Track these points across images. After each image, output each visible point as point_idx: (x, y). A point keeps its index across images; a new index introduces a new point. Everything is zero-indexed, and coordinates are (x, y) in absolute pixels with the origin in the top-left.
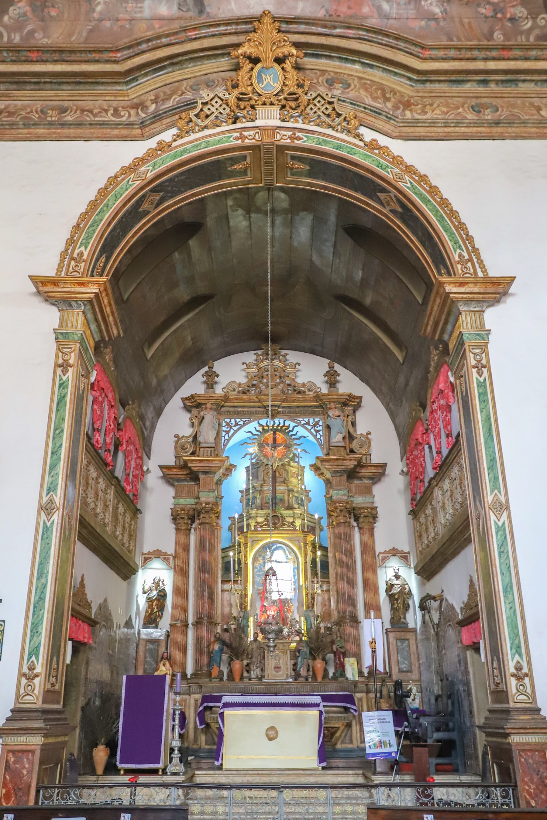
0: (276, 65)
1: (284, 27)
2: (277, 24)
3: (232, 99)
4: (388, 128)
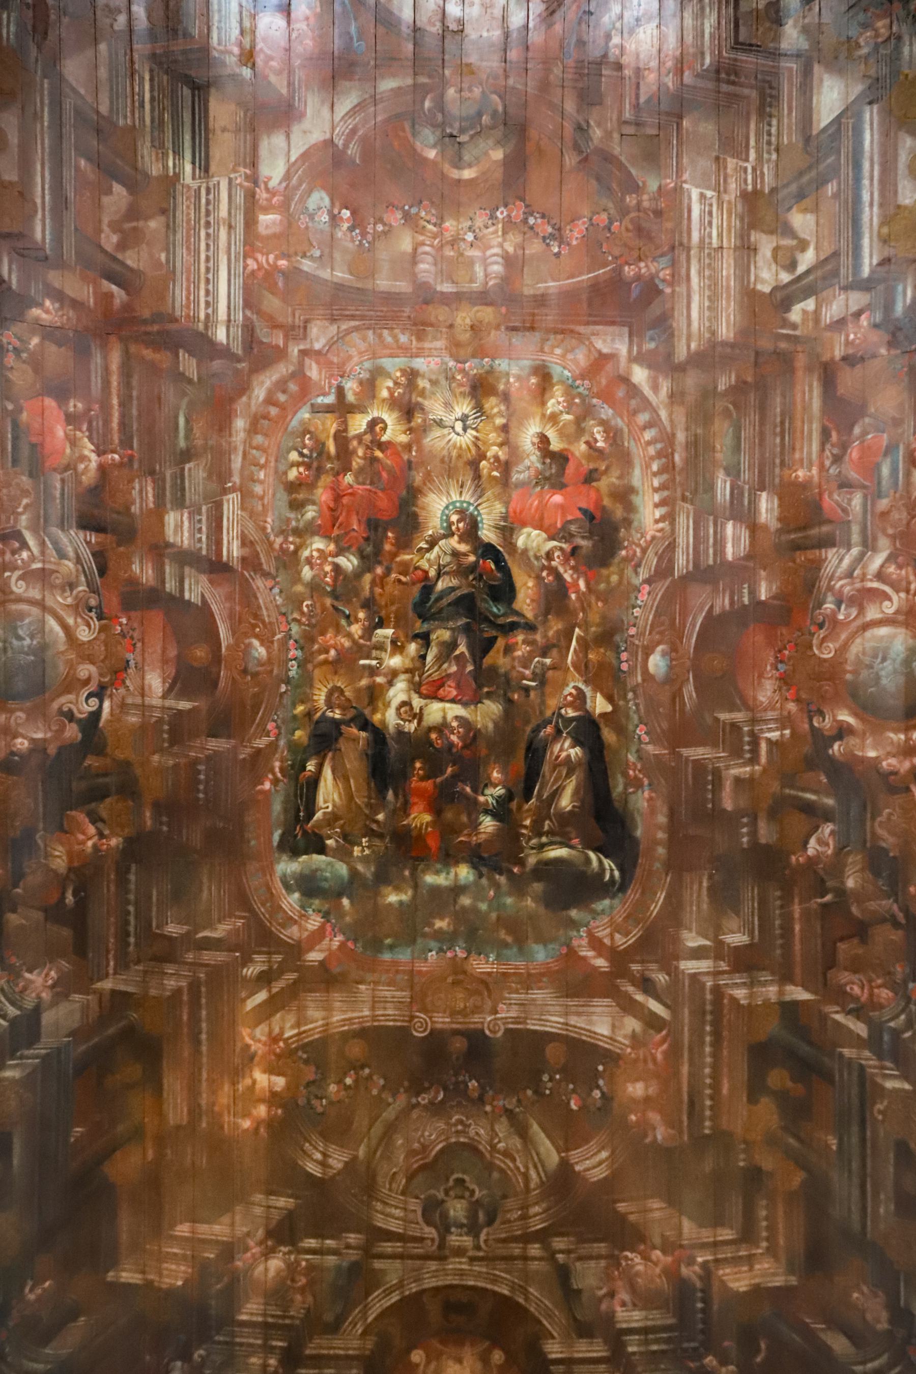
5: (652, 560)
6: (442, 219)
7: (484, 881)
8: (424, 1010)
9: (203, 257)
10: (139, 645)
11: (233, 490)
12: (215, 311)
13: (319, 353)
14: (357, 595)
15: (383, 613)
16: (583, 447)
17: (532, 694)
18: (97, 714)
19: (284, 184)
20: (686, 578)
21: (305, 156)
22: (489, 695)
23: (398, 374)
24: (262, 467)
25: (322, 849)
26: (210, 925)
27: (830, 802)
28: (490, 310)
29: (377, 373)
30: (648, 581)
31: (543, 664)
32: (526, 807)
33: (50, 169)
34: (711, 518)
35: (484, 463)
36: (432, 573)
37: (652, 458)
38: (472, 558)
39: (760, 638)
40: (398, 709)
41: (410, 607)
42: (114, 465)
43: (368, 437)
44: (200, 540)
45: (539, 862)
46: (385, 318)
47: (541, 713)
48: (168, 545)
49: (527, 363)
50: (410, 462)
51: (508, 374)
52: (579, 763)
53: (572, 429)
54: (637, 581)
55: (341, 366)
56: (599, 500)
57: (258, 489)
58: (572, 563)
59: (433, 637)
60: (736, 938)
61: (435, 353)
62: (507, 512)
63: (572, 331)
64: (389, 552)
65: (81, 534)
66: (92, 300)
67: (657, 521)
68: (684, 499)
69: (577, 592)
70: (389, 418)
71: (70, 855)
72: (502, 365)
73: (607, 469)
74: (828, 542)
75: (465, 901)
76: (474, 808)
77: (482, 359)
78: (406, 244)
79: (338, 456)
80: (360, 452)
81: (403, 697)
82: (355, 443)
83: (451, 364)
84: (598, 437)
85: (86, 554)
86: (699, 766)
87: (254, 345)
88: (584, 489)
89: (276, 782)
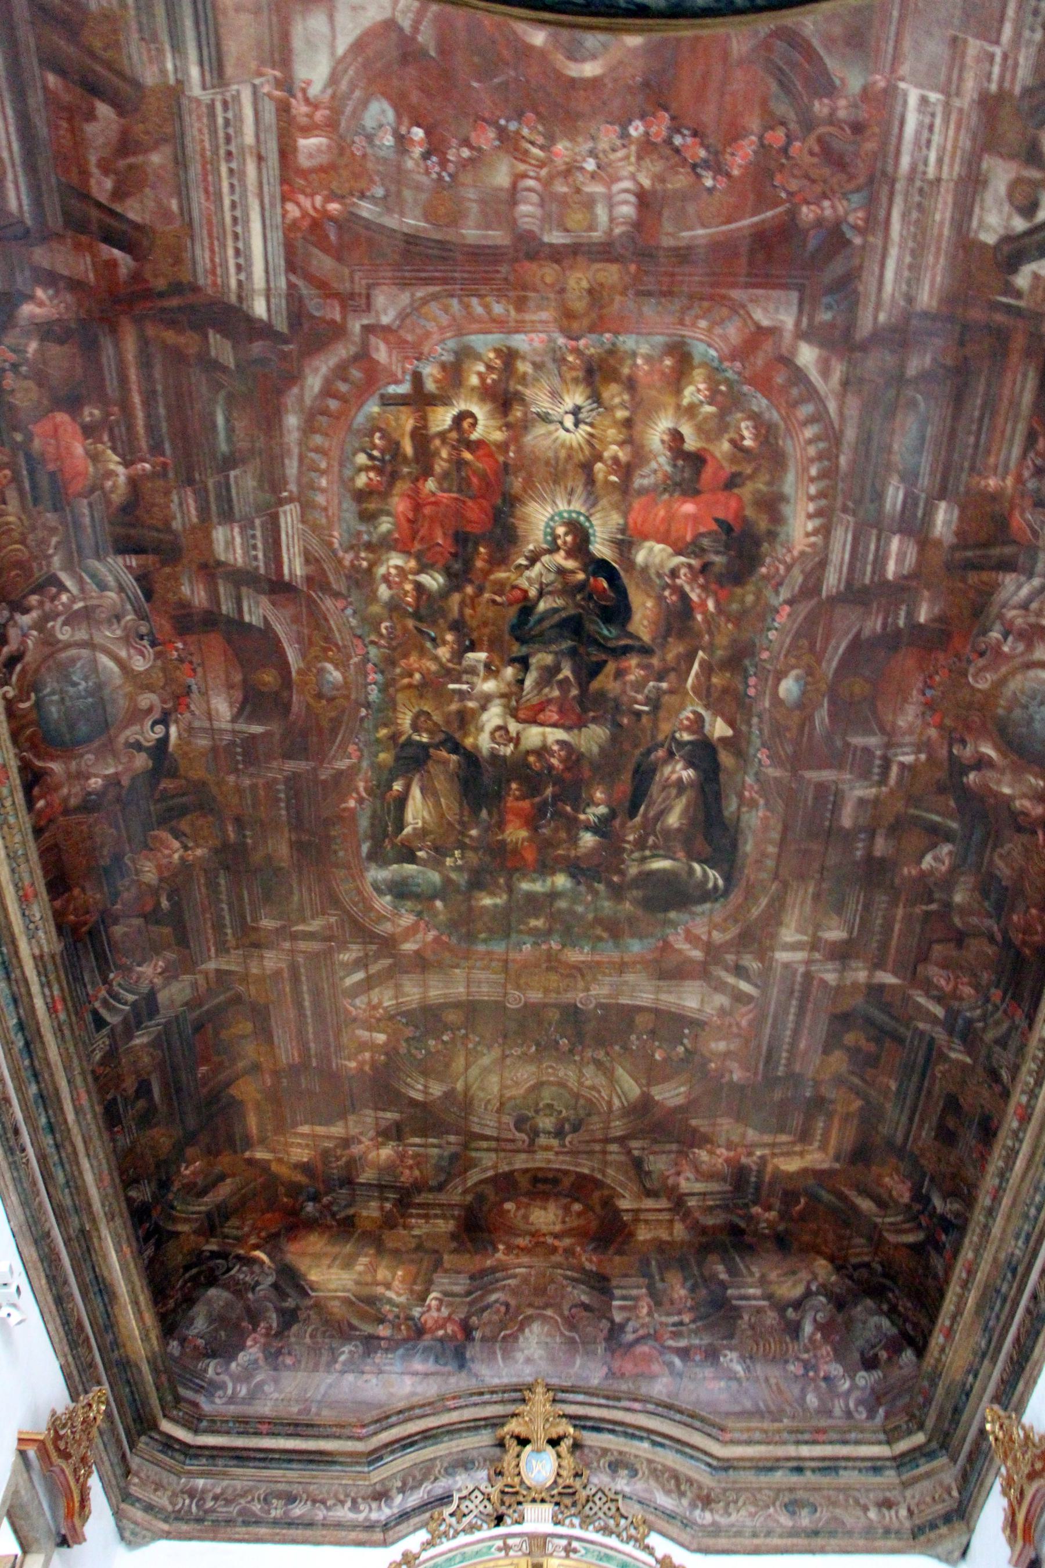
0: (549, 1448)
1: (561, 1396)
2: (551, 1394)
3: (495, 1496)
4: (685, 1537)
5: (797, 577)
6: (552, 138)
7: (582, 888)
8: (518, 987)
9: (227, 203)
10: (199, 670)
11: (290, 500)
12: (250, 276)
13: (387, 329)
14: (444, 617)
15: (475, 635)
16: (726, 446)
17: (644, 719)
18: (164, 740)
19: (329, 91)
20: (833, 600)
21: (358, 46)
22: (594, 720)
23: (492, 355)
24: (323, 473)
25: (412, 859)
26: (304, 920)
27: (955, 825)
28: (614, 268)
29: (465, 354)
30: (790, 602)
31: (658, 689)
32: (630, 824)
33: (12, 101)
34: (875, 532)
35: (599, 466)
36: (533, 593)
37: (812, 461)
38: (581, 576)
39: (910, 663)
40: (492, 734)
41: (506, 628)
42: (146, 476)
43: (454, 435)
44: (256, 558)
45: (640, 873)
46: (475, 281)
47: (653, 737)
48: (219, 564)
49: (660, 339)
50: (506, 465)
51: (634, 355)
52: (692, 784)
53: (712, 424)
54: (775, 602)
55: (417, 346)
56: (741, 508)
57: (321, 499)
58: (701, 580)
59: (533, 661)
60: (835, 934)
61: (539, 327)
62: (626, 524)
63: (723, 297)
64: (482, 570)
65: (120, 559)
66: (91, 276)
67: (808, 535)
68: (845, 510)
69: (705, 612)
70: (480, 411)
71: (159, 868)
72: (628, 342)
73: (756, 470)
74: (1007, 565)
75: (562, 904)
76: (573, 826)
77: (601, 334)
78: (501, 176)
79: (417, 459)
80: (444, 454)
81: (497, 721)
82: (437, 442)
83: (561, 341)
84: (746, 433)
85: (129, 580)
86: (821, 788)
87: (304, 320)
88: (722, 496)
89: (361, 801)
